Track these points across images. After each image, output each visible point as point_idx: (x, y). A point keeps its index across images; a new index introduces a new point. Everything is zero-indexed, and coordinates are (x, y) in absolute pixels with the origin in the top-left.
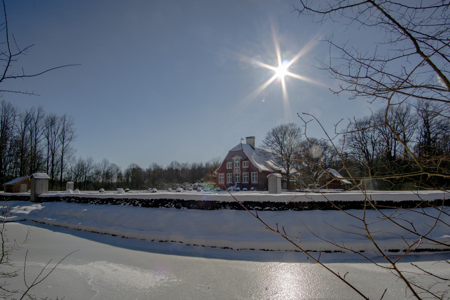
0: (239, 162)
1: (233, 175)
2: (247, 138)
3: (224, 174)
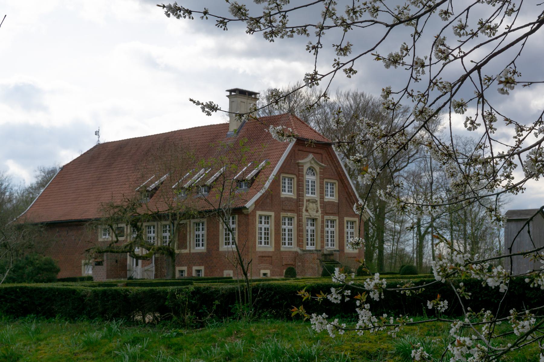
1: (299, 221)
3: (272, 214)
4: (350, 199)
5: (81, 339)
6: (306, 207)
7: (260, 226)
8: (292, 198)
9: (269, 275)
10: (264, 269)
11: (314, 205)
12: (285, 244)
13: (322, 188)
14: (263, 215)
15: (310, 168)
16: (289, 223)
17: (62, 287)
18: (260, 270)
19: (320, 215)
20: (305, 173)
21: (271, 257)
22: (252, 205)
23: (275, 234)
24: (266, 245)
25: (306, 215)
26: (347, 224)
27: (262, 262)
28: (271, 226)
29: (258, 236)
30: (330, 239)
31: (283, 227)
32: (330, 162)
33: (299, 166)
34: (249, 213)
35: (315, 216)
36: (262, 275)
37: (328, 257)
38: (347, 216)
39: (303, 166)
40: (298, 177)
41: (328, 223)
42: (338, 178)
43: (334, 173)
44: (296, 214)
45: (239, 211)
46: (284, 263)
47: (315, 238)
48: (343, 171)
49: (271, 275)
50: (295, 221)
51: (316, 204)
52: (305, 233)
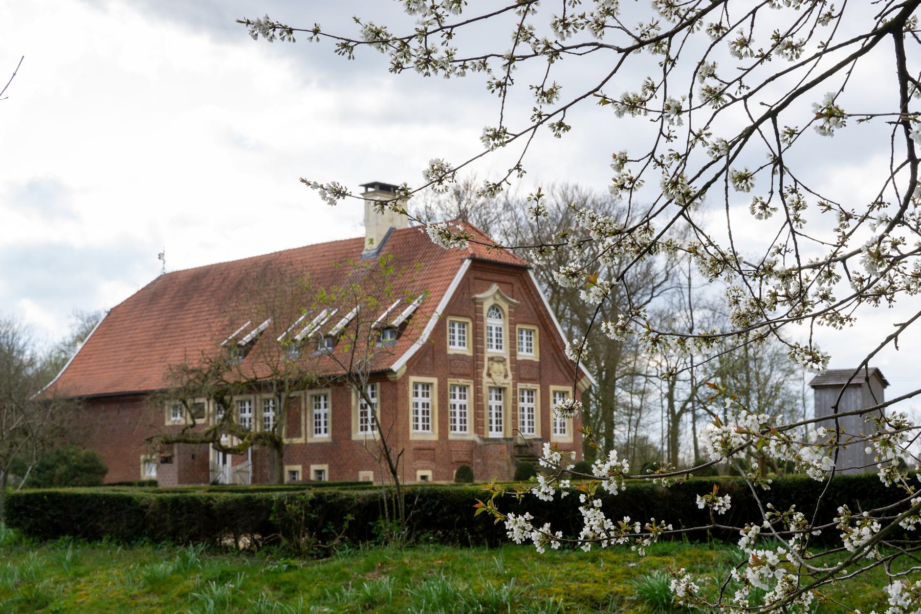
1: (478, 391)
3: (435, 380)
4: (559, 356)
5: (142, 575)
6: (489, 370)
7: (415, 399)
8: (465, 355)
9: (430, 479)
10: (423, 468)
11: (501, 366)
12: (455, 429)
13: (512, 338)
14: (420, 383)
15: (493, 307)
16: (460, 395)
17: (111, 493)
18: (416, 470)
19: (511, 383)
20: (485, 315)
21: (434, 450)
22: (402, 367)
23: (440, 413)
24: (426, 431)
25: (488, 383)
26: (555, 396)
27: (419, 458)
28: (433, 399)
29: (412, 416)
30: (526, 420)
31: (452, 401)
32: (526, 297)
33: (476, 304)
34: (398, 378)
35: (503, 384)
36: (419, 479)
37: (525, 449)
38: (554, 383)
39: (482, 304)
40: (474, 321)
41: (523, 394)
42: (539, 323)
43: (532, 314)
44: (472, 381)
45: (381, 376)
46: (454, 459)
47: (503, 418)
48: (546, 311)
49: (434, 479)
50: (470, 392)
51: (504, 365)
52: (487, 412)
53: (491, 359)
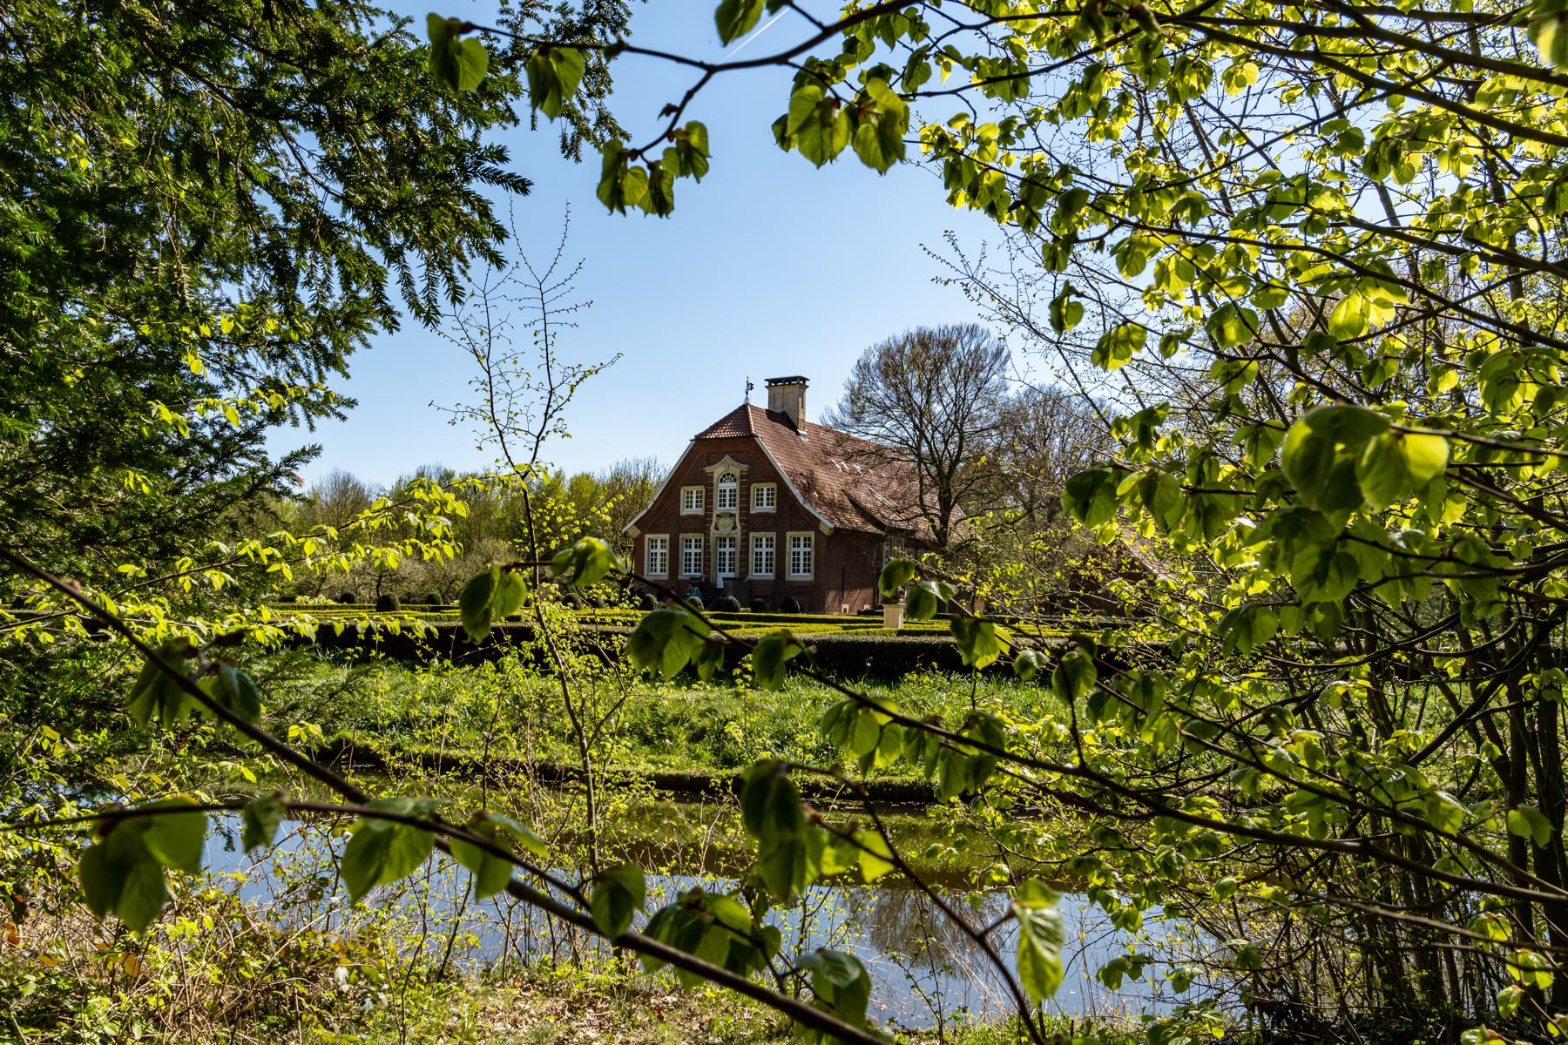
0: (734, 485)
1: (707, 541)
2: (773, 383)
11: (728, 521)
53: (719, 516)
